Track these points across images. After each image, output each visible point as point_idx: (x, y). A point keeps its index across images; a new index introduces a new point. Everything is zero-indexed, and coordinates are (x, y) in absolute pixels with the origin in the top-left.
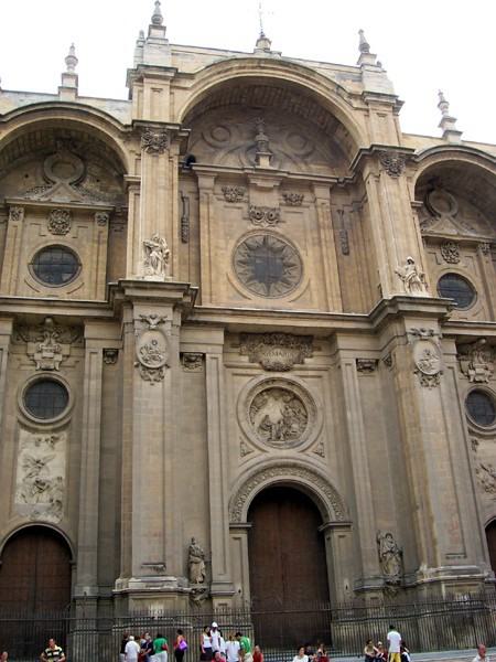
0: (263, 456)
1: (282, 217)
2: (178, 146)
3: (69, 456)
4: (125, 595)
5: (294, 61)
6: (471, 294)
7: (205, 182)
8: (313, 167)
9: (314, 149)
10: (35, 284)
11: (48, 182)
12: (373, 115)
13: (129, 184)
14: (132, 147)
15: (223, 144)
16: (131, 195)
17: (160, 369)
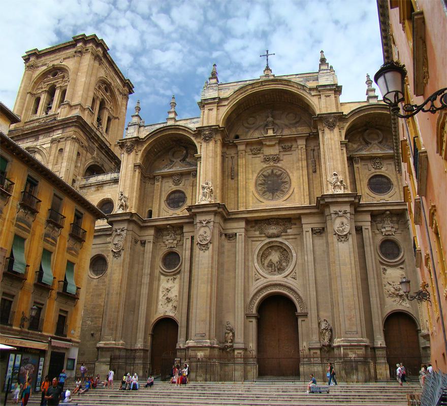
0: (265, 280)
1: (281, 158)
2: (219, 135)
3: (180, 285)
4: (188, 348)
5: (279, 78)
6: (389, 185)
7: (241, 148)
8: (299, 128)
9: (301, 118)
10: (167, 209)
11: (172, 161)
12: (323, 97)
13: (198, 158)
14: (199, 140)
15: (252, 126)
16: (199, 163)
17: (207, 244)
